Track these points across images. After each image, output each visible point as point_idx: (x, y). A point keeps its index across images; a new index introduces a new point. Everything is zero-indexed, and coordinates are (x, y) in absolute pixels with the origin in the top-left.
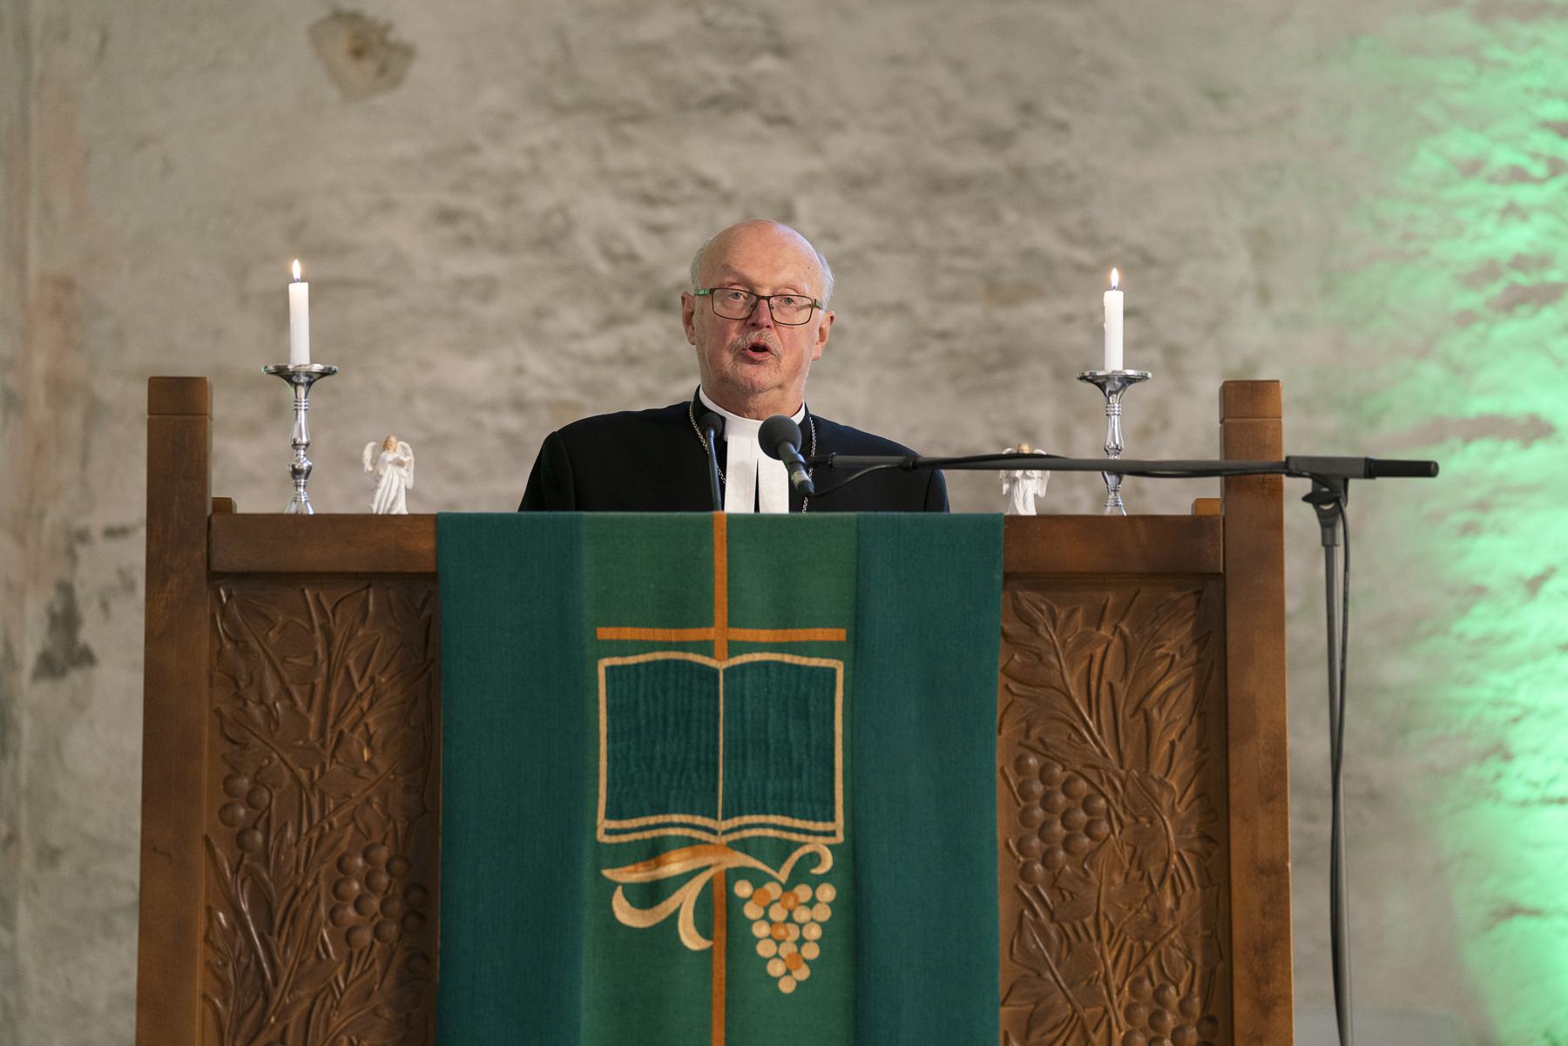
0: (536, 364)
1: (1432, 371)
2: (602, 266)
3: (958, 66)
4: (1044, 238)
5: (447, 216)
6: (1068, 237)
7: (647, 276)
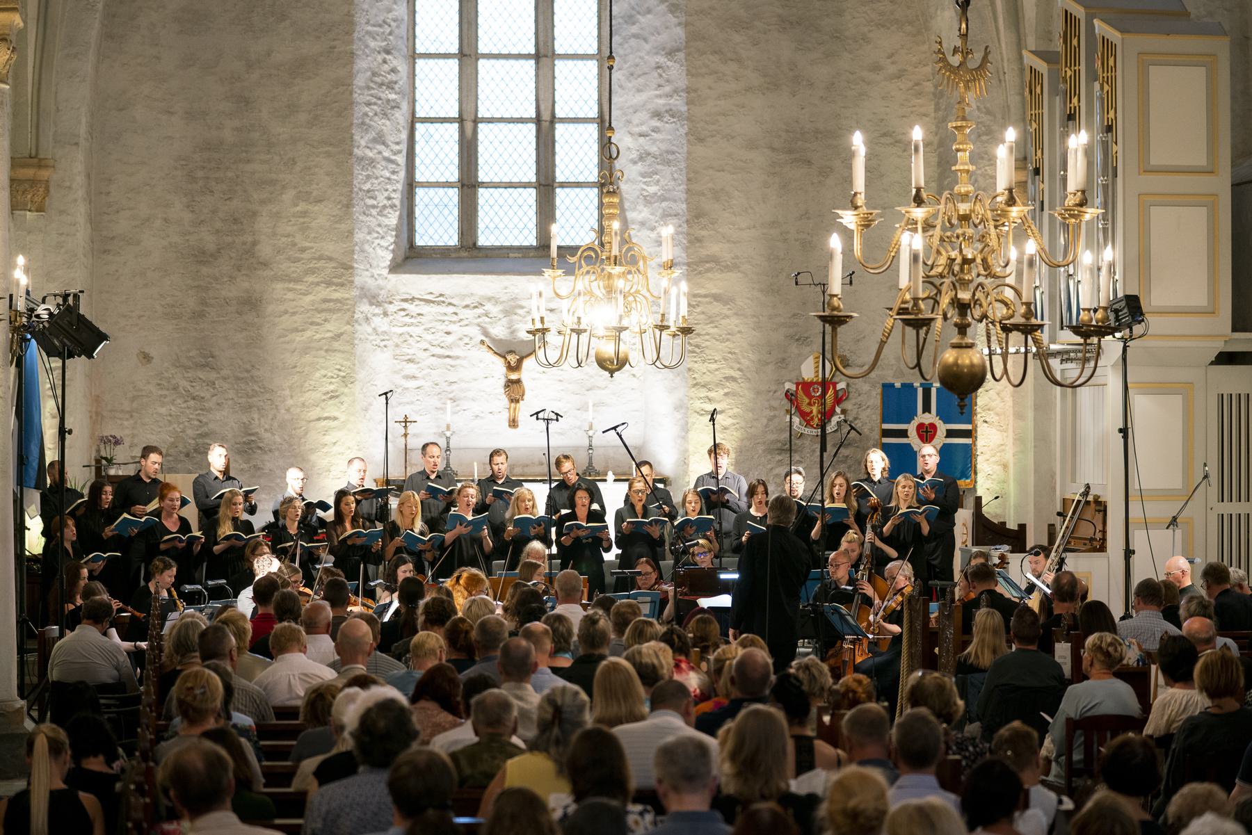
0: (173, 408)
1: (318, 409)
3: (241, 359)
4: (256, 388)
5: (159, 385)
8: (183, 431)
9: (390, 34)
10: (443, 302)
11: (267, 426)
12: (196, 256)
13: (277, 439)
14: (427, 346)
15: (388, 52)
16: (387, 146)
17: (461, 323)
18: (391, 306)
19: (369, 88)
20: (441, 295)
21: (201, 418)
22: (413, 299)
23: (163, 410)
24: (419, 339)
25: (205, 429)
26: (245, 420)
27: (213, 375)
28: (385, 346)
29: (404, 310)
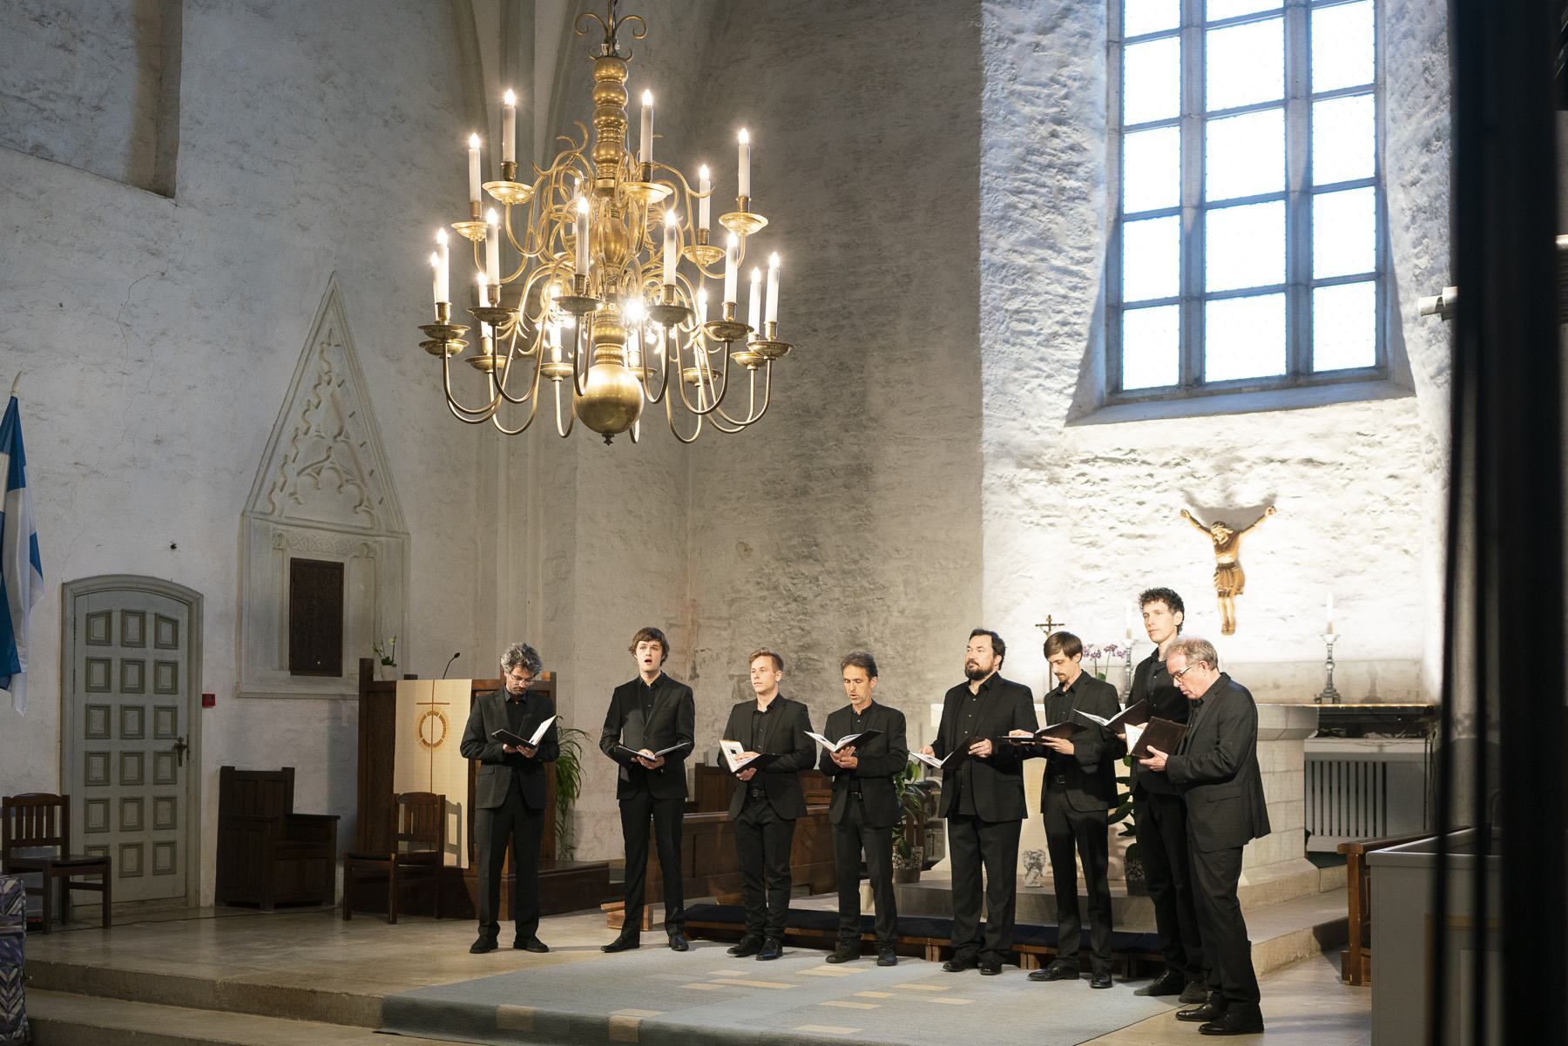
0: (773, 614)
2: (784, 592)
3: (849, 547)
5: (758, 583)
6: (870, 583)
7: (792, 594)
8: (785, 643)
9: (1066, 97)
10: (1135, 460)
11: (877, 634)
12: (799, 416)
13: (890, 651)
14: (1114, 523)
15: (1060, 122)
16: (1060, 251)
17: (1159, 488)
18: (1067, 470)
19: (1018, 170)
20: (1132, 451)
21: (803, 625)
22: (1095, 459)
23: (762, 616)
24: (1103, 513)
25: (807, 640)
26: (852, 627)
27: (818, 568)
28: (1051, 525)
29: (1083, 474)
